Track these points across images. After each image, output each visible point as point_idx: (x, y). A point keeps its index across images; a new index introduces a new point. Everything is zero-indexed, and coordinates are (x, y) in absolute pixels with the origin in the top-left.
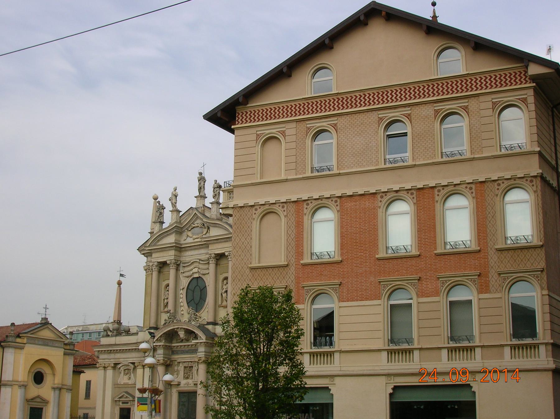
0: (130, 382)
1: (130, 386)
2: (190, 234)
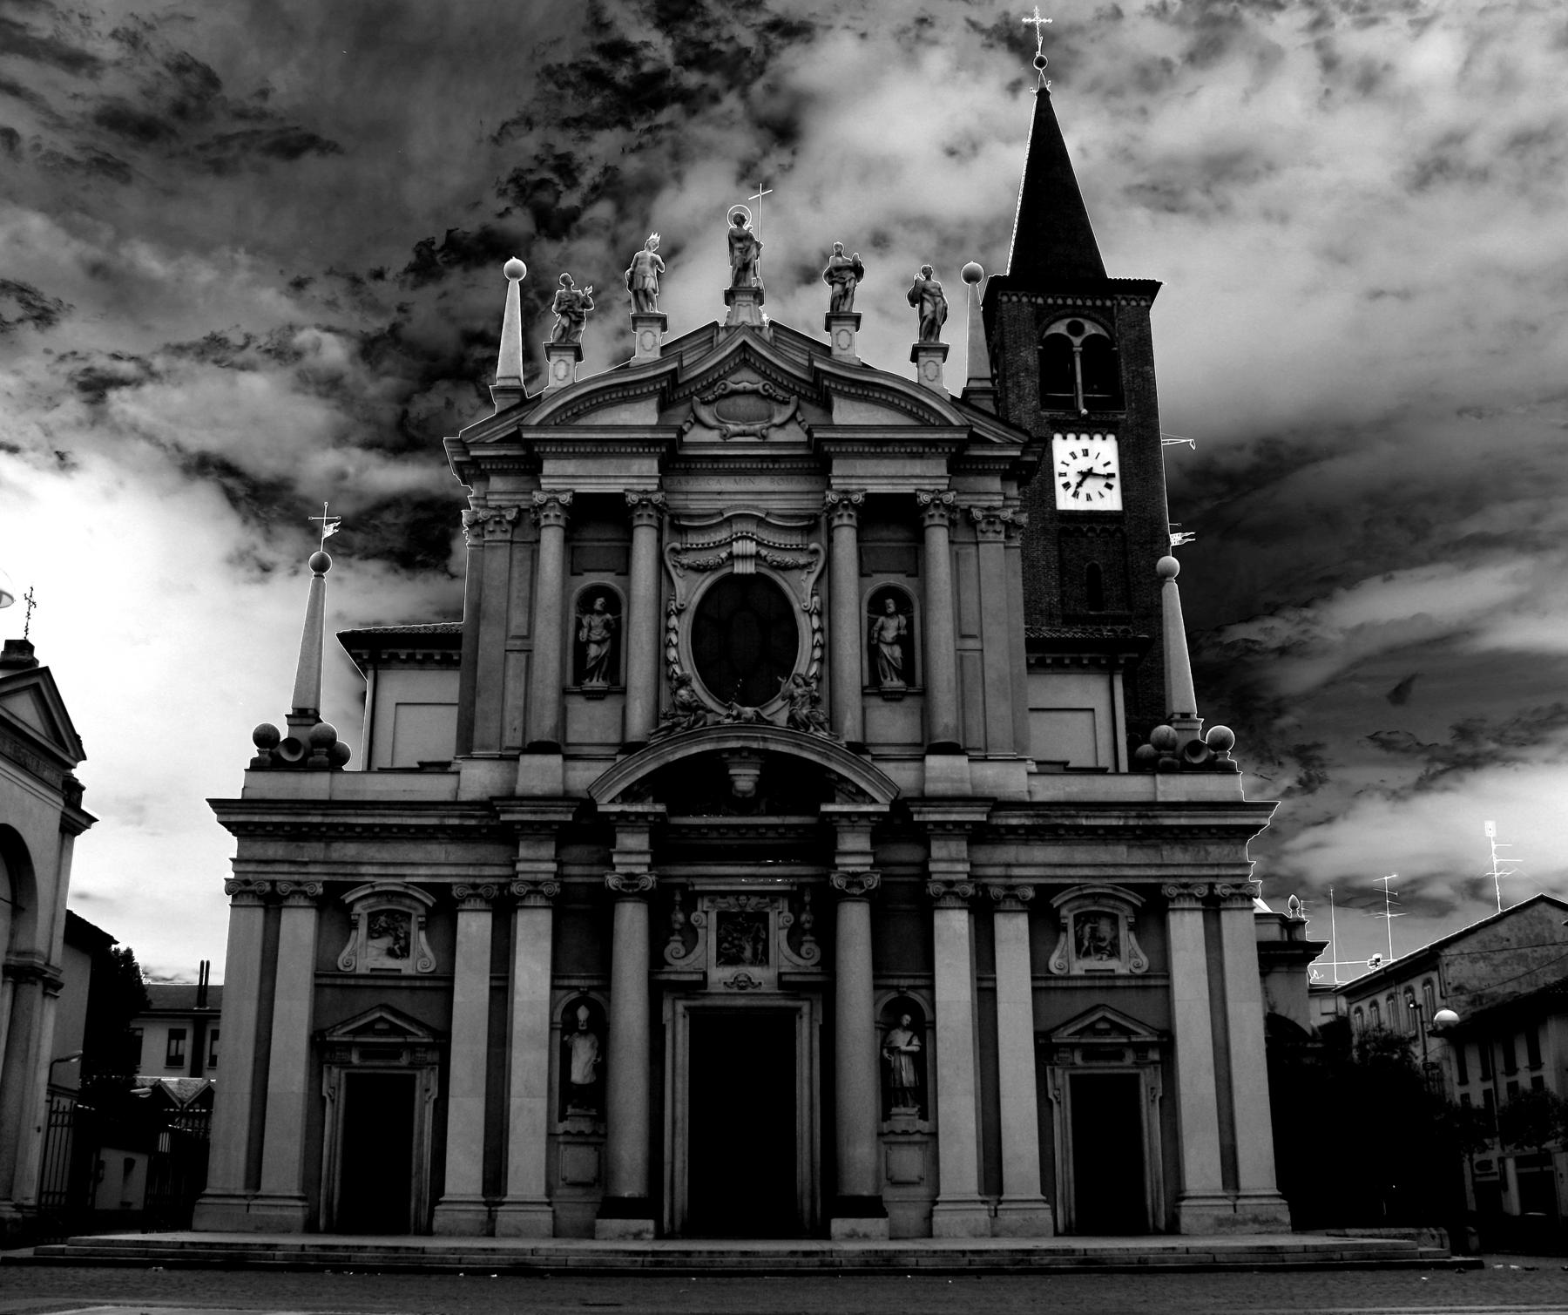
0: (406, 966)
1: (404, 983)
2: (705, 414)
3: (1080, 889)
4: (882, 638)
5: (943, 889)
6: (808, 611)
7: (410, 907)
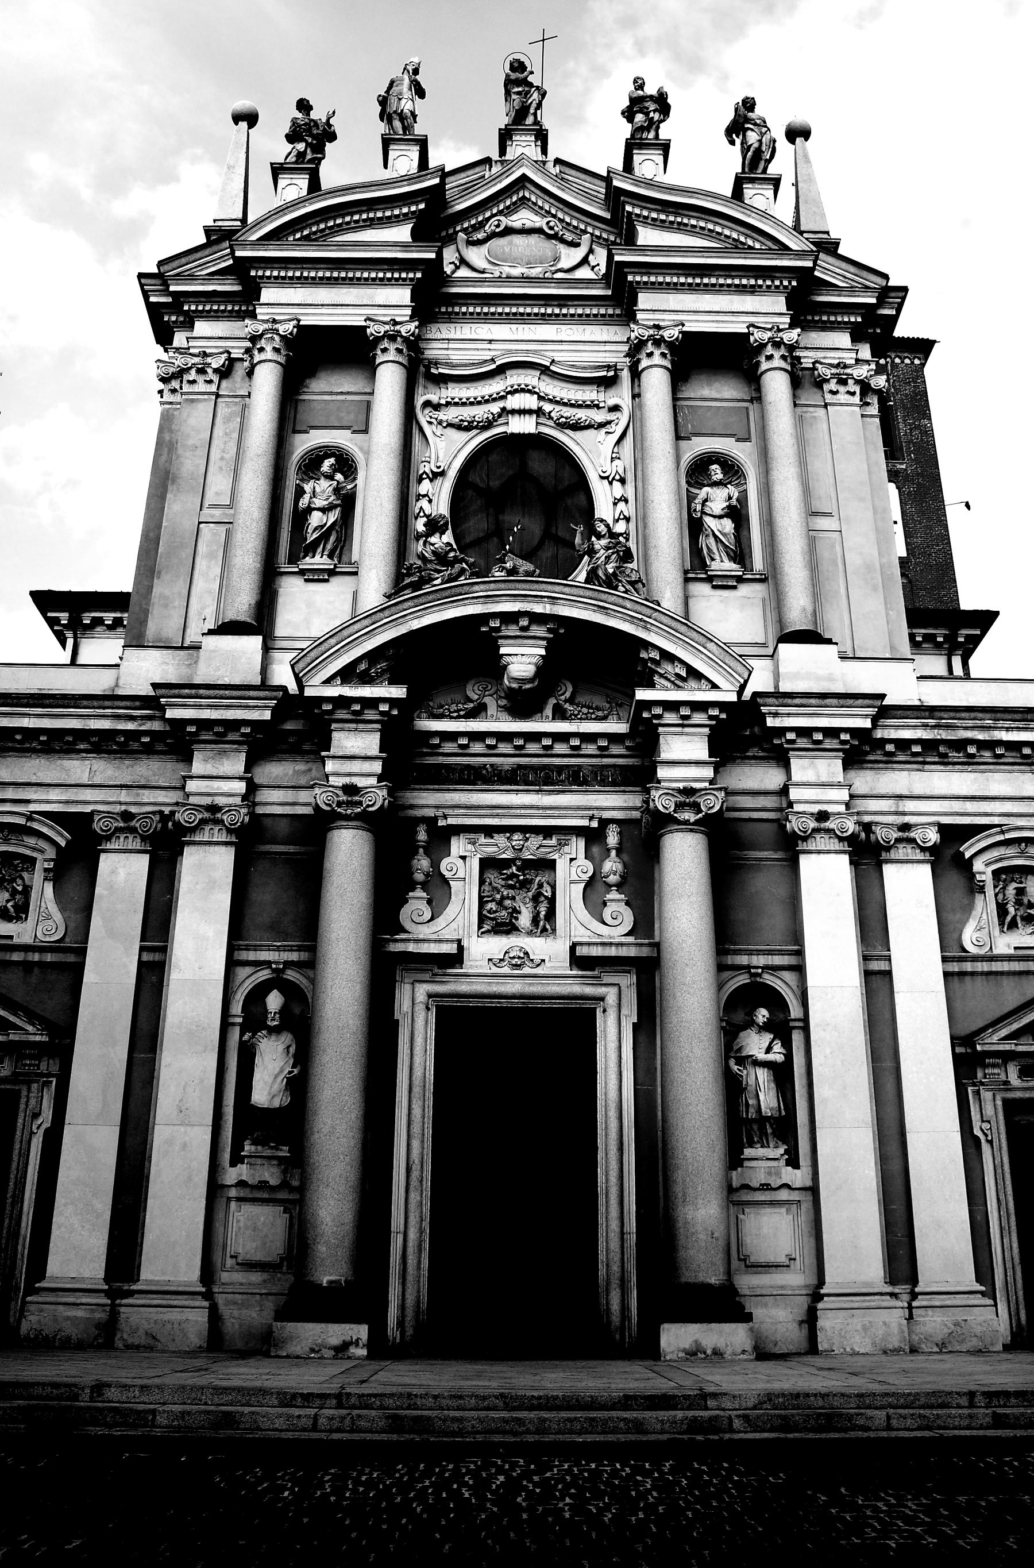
3: (1003, 832)
4: (707, 510)
5: (812, 824)
6: (607, 478)
7: (34, 849)
